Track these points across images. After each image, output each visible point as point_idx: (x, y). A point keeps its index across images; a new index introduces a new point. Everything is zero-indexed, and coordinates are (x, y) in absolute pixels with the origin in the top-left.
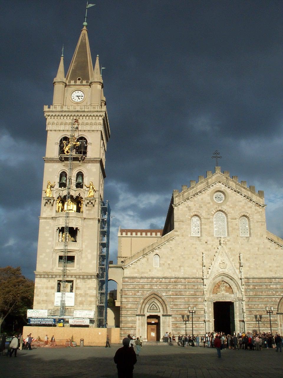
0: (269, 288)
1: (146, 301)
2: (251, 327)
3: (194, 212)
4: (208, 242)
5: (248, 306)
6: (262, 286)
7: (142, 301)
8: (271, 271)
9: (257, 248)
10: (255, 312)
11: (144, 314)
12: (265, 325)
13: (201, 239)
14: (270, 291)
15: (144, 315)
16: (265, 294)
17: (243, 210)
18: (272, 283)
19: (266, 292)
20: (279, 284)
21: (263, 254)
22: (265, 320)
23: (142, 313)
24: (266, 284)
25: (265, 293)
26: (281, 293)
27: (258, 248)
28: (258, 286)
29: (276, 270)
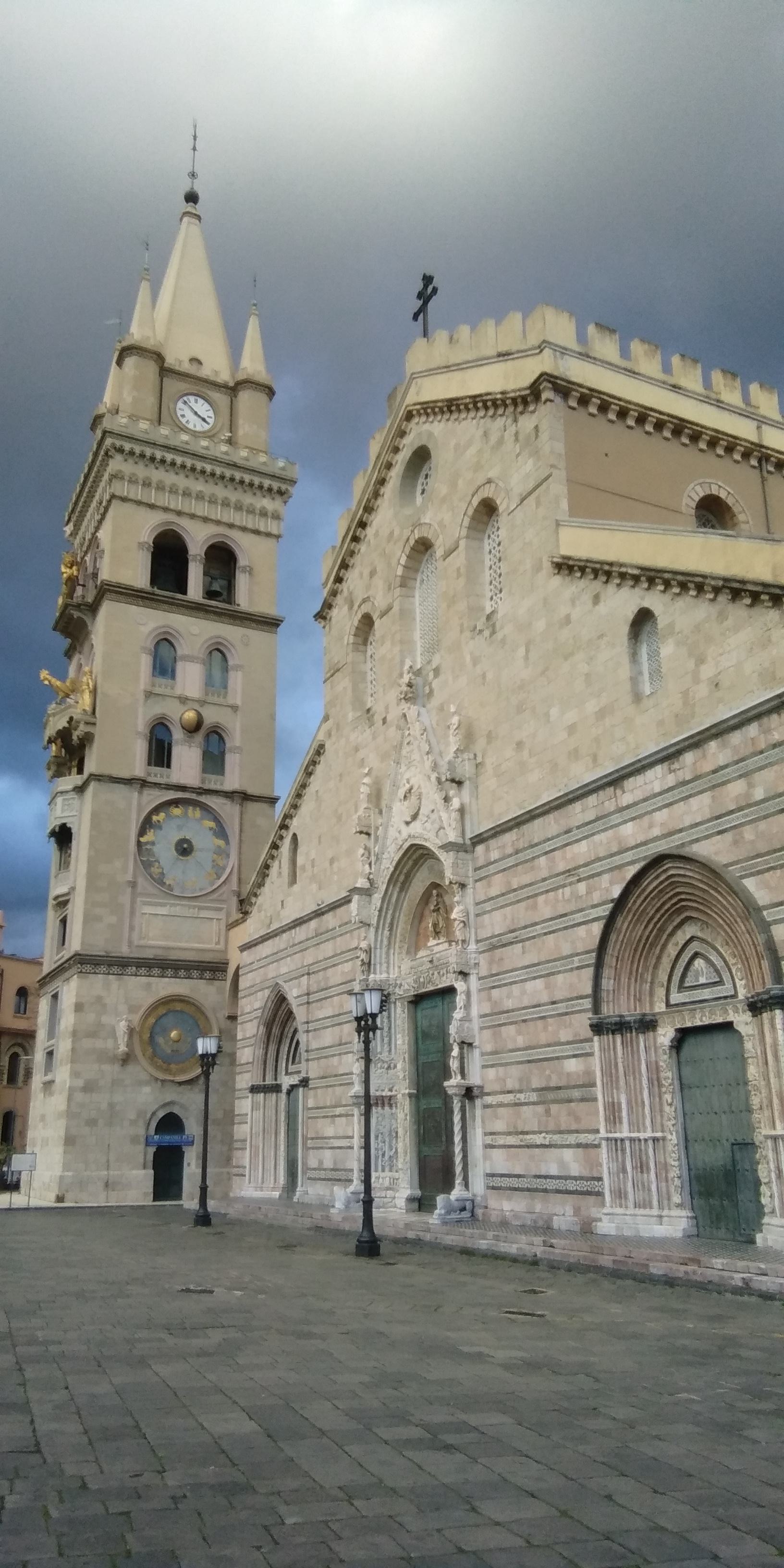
0: (561, 867)
1: (276, 1031)
2: (499, 1126)
3: (359, 606)
4: (388, 719)
5: (490, 999)
6: (536, 861)
7: (262, 1029)
8: (575, 755)
9: (522, 651)
10: (512, 1029)
11: (278, 1082)
12: (548, 1112)
13: (373, 716)
14: (564, 886)
15: (277, 1089)
16: (547, 913)
17: (481, 479)
18: (575, 832)
19: (551, 894)
20: (599, 825)
21: (543, 673)
22: (550, 1076)
23: (269, 1081)
24: (547, 846)
25: (546, 902)
26: (612, 883)
27: (527, 651)
28: (520, 867)
29: (597, 740)
